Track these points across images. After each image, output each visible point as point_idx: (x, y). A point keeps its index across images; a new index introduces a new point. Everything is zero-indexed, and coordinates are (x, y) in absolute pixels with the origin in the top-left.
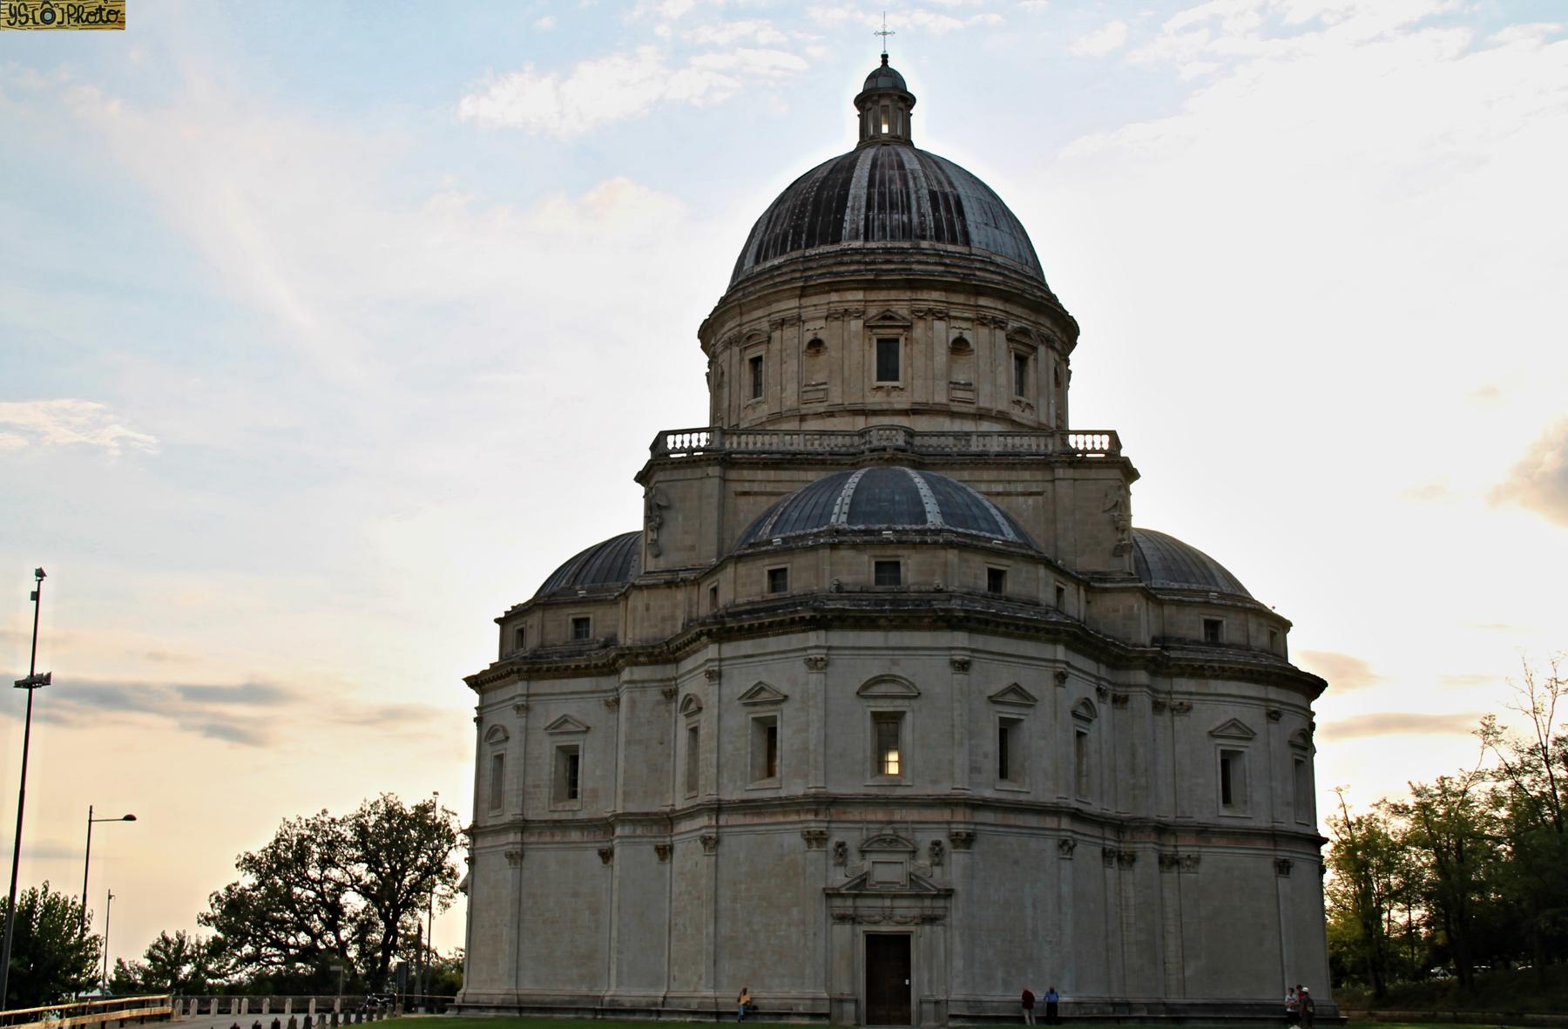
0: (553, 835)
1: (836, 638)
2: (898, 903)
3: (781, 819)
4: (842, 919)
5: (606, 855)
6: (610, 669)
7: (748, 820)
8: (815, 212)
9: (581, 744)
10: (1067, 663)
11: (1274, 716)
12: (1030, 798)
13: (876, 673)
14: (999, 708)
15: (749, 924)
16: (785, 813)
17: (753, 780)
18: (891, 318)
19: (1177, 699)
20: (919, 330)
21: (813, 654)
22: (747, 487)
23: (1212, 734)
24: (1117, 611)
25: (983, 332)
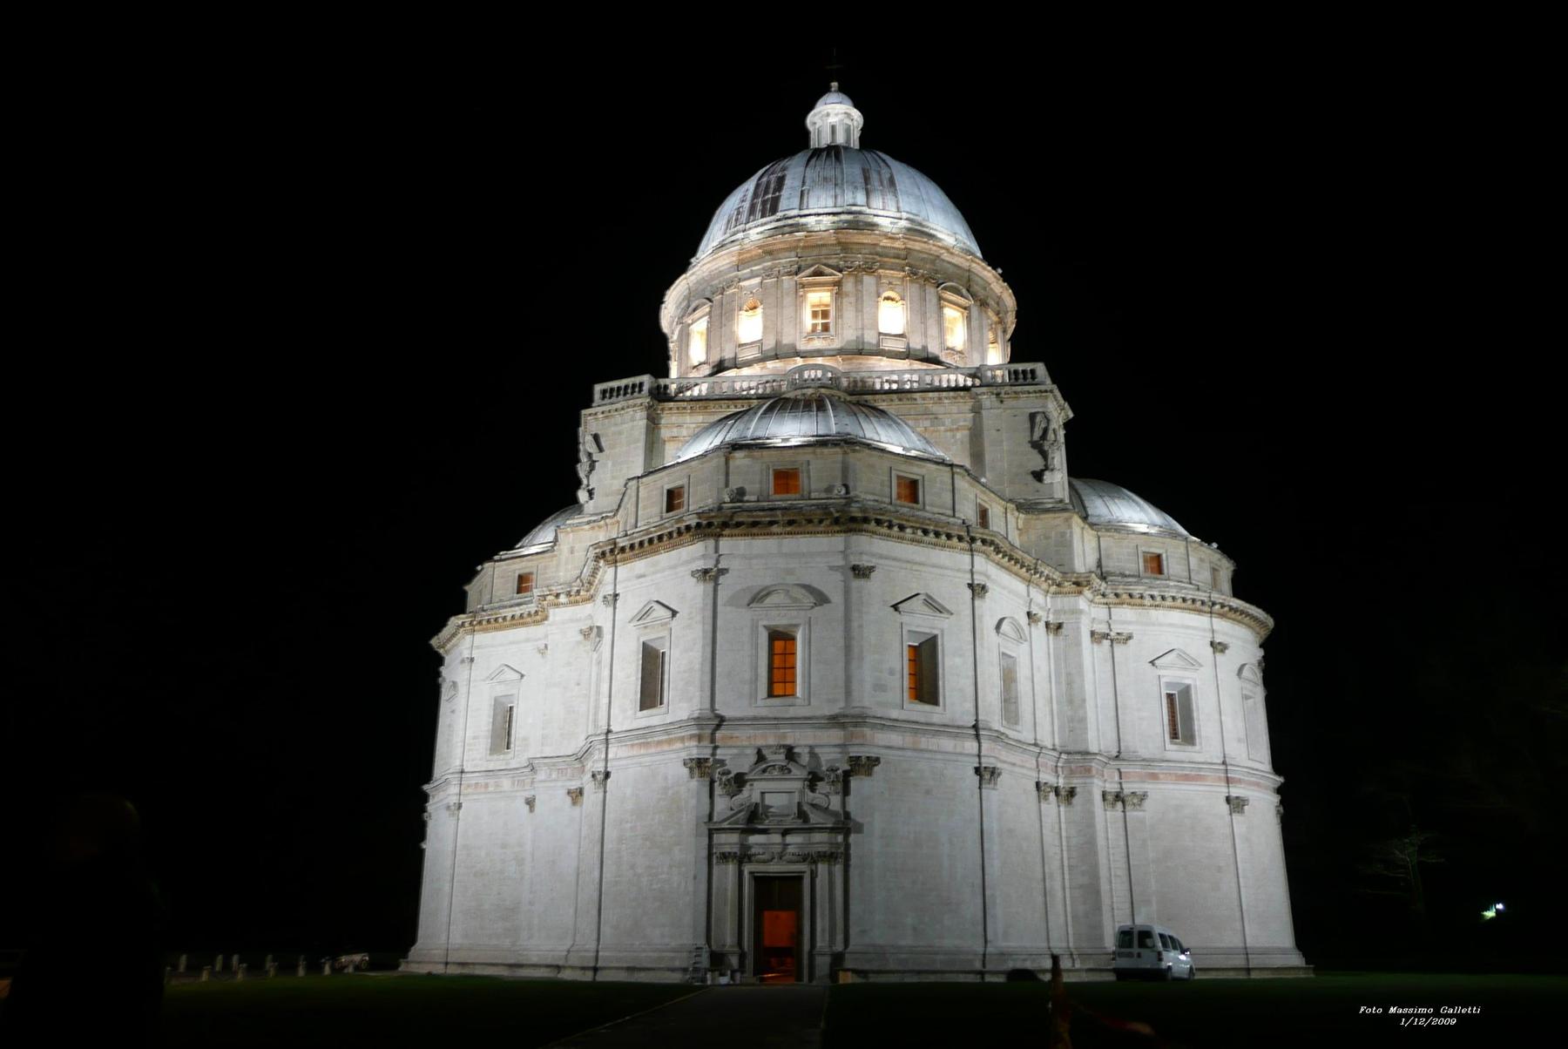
0: (487, 786)
1: (726, 544)
2: (789, 839)
3: (666, 748)
4: (725, 857)
5: (530, 803)
6: (539, 617)
7: (635, 752)
8: (755, 195)
9: (514, 691)
10: (988, 577)
11: (1218, 647)
12: (946, 721)
13: (768, 582)
14: (905, 618)
15: (633, 867)
16: (670, 742)
17: (642, 709)
18: (821, 274)
19: (1116, 628)
20: (849, 286)
21: (700, 565)
22: (675, 432)
23: (1152, 662)
24: (1047, 538)
25: (913, 289)
